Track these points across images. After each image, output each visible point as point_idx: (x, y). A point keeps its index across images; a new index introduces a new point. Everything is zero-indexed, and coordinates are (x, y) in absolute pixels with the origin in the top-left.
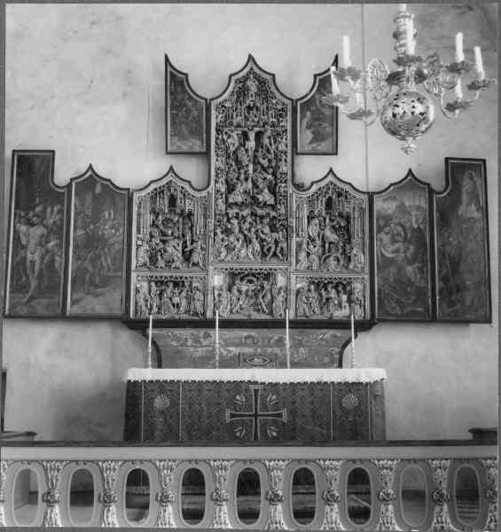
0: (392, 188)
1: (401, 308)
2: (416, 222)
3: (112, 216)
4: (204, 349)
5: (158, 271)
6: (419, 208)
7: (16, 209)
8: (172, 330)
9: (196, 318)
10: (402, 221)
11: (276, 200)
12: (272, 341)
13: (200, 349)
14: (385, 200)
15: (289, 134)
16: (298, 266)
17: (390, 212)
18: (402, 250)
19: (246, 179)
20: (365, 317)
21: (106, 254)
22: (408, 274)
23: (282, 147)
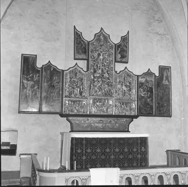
2: (151, 85)
3: (57, 78)
4: (87, 124)
5: (72, 98)
6: (151, 81)
7: (23, 75)
8: (77, 118)
9: (84, 114)
11: (109, 76)
12: (108, 122)
13: (85, 124)
14: (141, 78)
17: (143, 82)
18: (146, 94)
19: (100, 68)
21: (54, 92)
22: (148, 101)
23: (111, 59)
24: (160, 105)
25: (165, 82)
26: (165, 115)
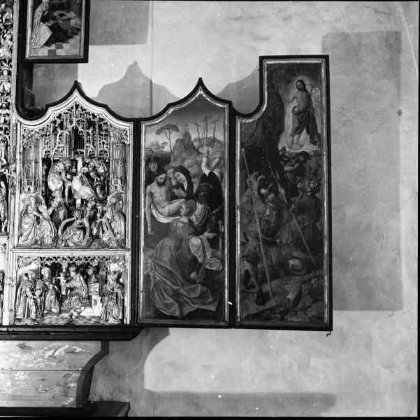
0: (171, 110)
1: (181, 306)
2: (208, 165)
6: (212, 142)
10: (186, 164)
14: (158, 132)
15: (15, 31)
16: (22, 239)
17: (167, 149)
18: (183, 211)
20: (122, 320)
24: (264, 265)
25: (292, 142)
26: (293, 319)
